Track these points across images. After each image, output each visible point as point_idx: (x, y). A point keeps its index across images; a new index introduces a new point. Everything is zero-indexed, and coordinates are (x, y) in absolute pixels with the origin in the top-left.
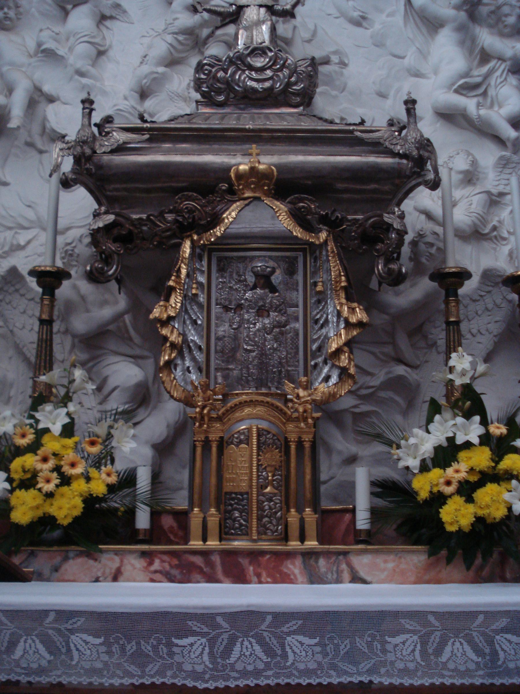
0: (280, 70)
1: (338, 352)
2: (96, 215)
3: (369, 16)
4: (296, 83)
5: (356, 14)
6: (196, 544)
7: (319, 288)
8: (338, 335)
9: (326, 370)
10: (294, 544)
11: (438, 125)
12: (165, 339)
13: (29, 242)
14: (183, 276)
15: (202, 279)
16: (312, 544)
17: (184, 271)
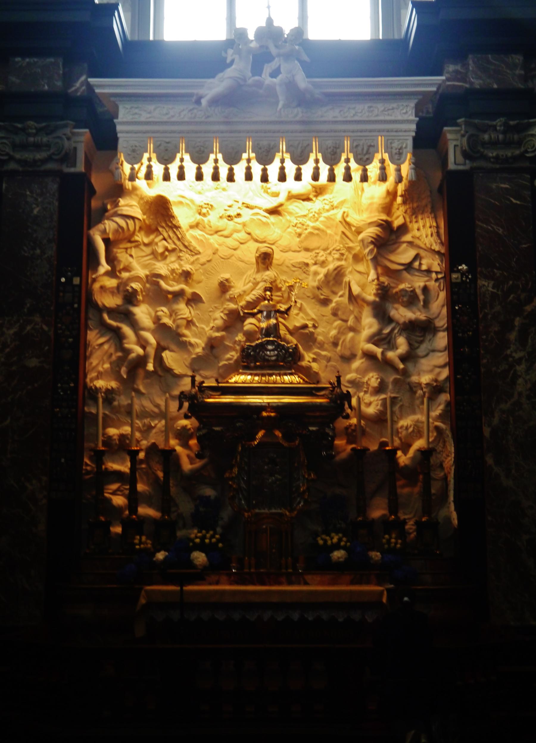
0: (281, 351)
1: (304, 492)
2: (199, 429)
3: (330, 298)
4: (288, 357)
5: (322, 297)
6: (246, 570)
7: (296, 465)
8: (303, 485)
9: (298, 499)
10: (284, 571)
11: (363, 360)
12: (231, 486)
13: (156, 425)
14: (238, 460)
15: (246, 460)
16: (290, 570)
17: (238, 457)
